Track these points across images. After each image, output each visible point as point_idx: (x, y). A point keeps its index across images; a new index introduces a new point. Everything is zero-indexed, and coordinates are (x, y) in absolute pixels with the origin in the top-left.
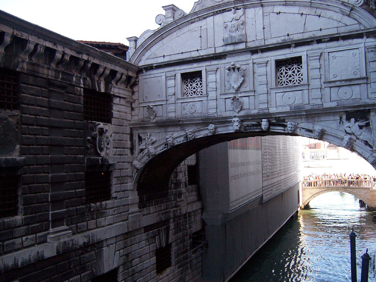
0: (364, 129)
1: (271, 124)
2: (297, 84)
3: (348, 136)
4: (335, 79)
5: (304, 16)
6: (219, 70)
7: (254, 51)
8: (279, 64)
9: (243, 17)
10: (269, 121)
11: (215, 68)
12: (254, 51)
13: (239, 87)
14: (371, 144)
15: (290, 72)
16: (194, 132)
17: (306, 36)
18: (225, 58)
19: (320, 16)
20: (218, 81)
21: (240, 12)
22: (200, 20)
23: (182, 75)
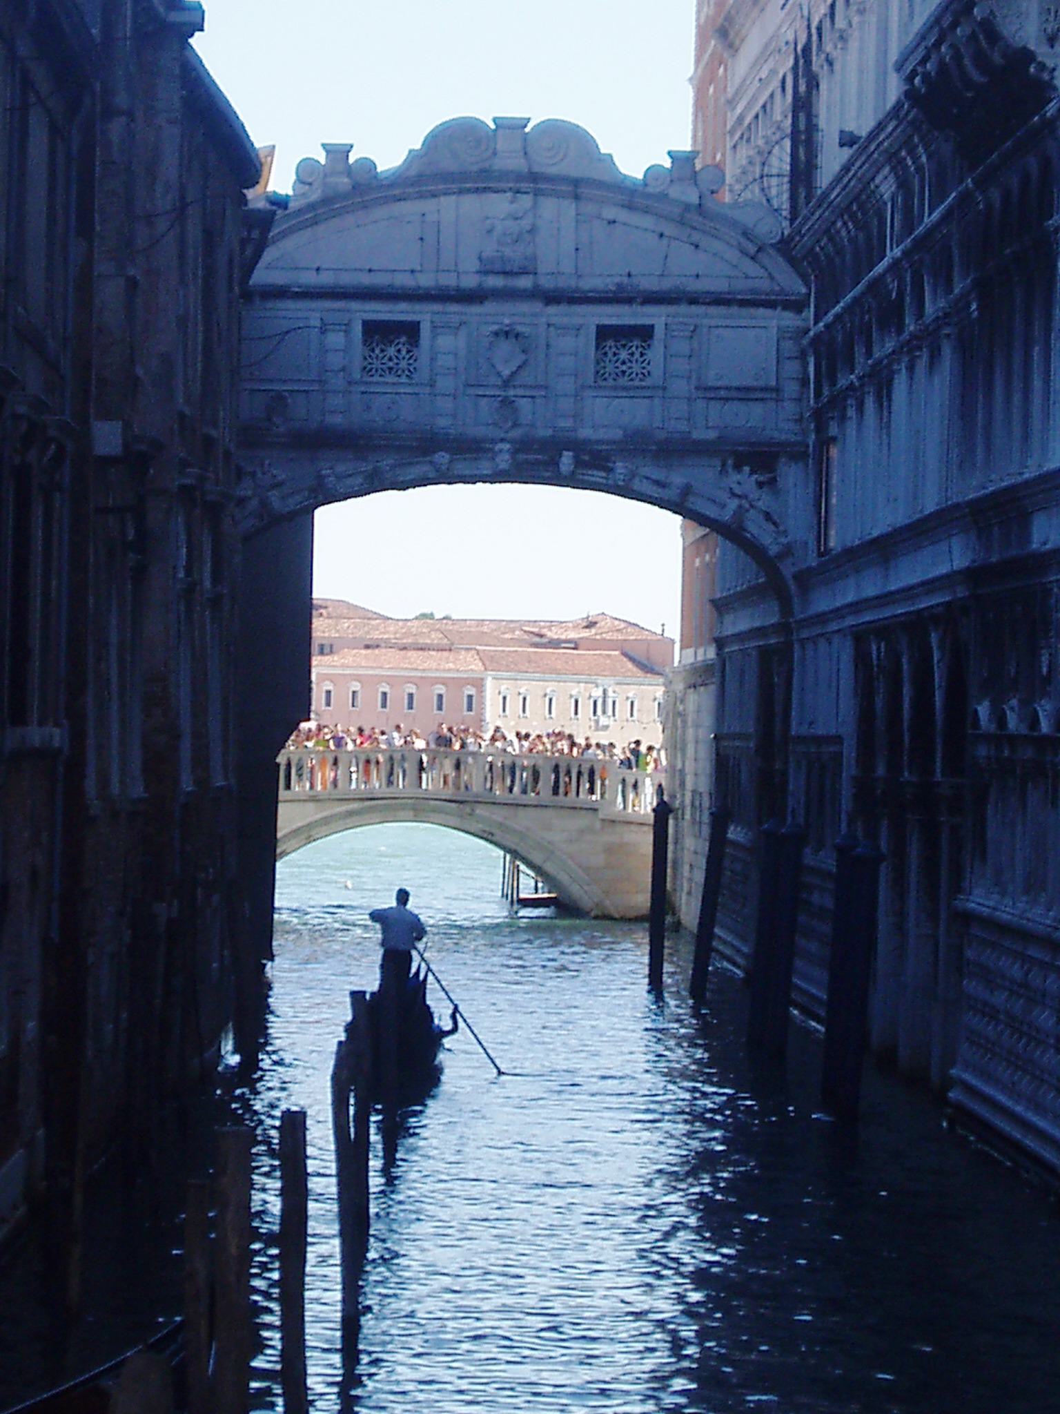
1: (579, 463)
2: (637, 383)
4: (719, 384)
5: (665, 241)
6: (463, 327)
7: (552, 298)
8: (603, 333)
11: (456, 319)
12: (552, 298)
13: (513, 374)
14: (775, 518)
15: (624, 355)
16: (393, 467)
17: (667, 284)
19: (697, 247)
21: (526, 201)
23: (365, 323)
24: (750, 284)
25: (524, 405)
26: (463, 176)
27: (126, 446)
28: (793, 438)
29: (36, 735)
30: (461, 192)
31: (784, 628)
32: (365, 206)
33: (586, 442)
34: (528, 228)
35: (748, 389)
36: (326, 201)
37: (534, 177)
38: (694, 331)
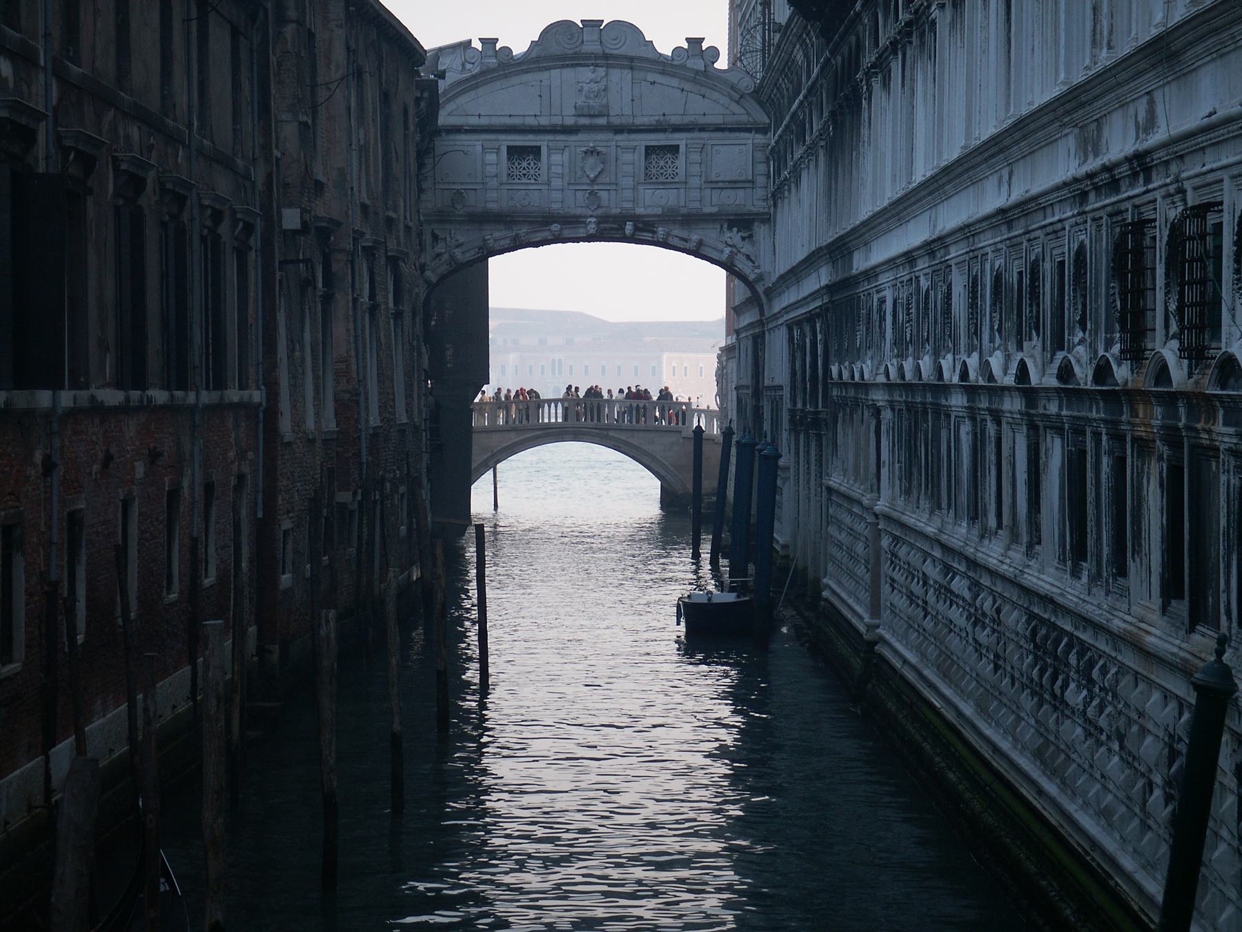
0: (747, 240)
1: (636, 229)
2: (670, 180)
3: (729, 249)
6: (567, 149)
8: (649, 150)
9: (605, 79)
10: (635, 225)
11: (562, 144)
12: (618, 130)
13: (596, 177)
14: (753, 258)
15: (662, 163)
16: (527, 233)
17: (686, 120)
18: (577, 134)
19: (704, 96)
20: (566, 164)
22: (539, 70)
23: (509, 148)
24: (735, 118)
25: (604, 195)
26: (564, 57)
27: (304, 223)
28: (762, 210)
29: (234, 395)
30: (563, 67)
31: (760, 323)
32: (506, 76)
33: (639, 216)
34: (603, 87)
35: (735, 182)
36: (482, 73)
37: (606, 57)
38: (702, 148)
